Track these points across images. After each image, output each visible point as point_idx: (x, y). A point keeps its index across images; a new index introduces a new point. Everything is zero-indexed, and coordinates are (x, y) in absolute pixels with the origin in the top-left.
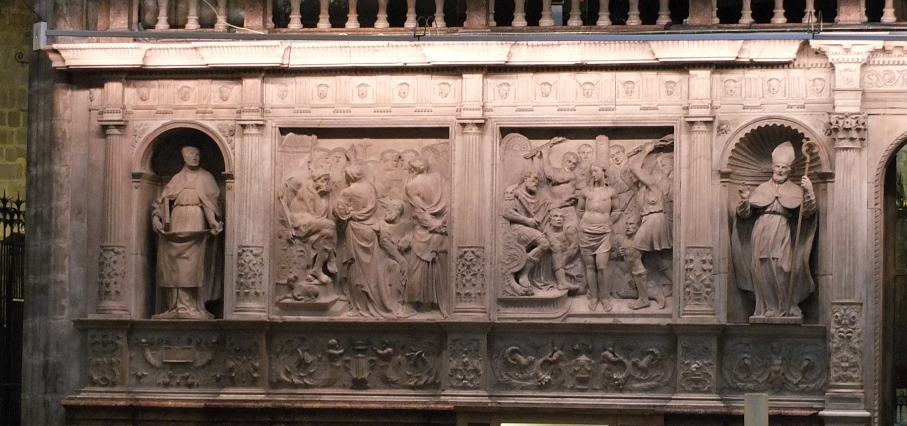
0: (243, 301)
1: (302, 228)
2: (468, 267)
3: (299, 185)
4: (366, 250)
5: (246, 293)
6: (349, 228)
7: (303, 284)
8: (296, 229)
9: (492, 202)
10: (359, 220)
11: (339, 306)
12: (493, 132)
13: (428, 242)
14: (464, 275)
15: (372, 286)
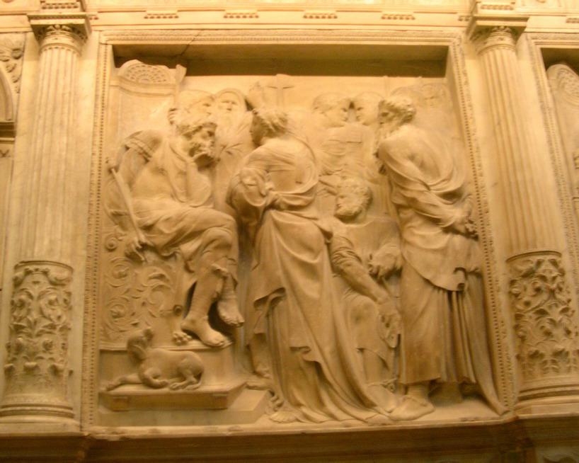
0: (21, 388)
1: (162, 227)
2: (552, 292)
3: (156, 142)
4: (311, 270)
5: (29, 371)
6: (268, 226)
7: (165, 349)
8: (148, 228)
9: (556, 174)
10: (291, 208)
11: (251, 400)
12: (531, 54)
13: (443, 251)
14: (542, 313)
15: (328, 349)
